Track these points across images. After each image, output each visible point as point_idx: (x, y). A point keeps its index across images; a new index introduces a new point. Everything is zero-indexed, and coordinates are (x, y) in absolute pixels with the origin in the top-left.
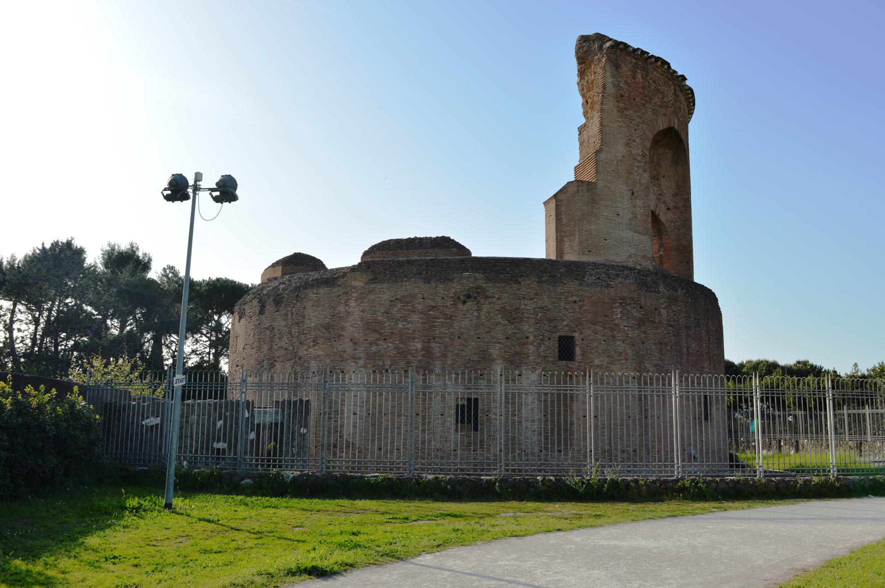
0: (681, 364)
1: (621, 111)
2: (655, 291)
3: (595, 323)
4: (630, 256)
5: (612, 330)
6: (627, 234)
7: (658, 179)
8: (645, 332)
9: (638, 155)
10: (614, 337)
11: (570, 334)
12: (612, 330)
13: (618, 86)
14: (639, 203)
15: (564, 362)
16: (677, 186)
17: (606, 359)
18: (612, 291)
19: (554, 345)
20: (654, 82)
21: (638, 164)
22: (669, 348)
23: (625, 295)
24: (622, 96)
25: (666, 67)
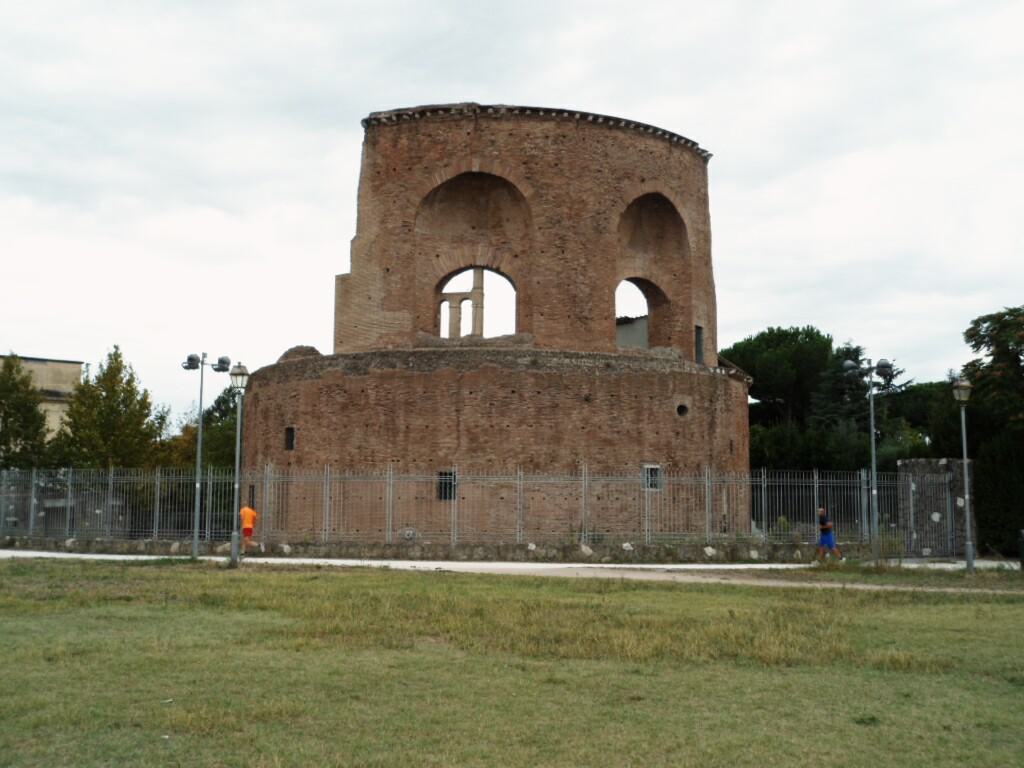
0: (394, 443)
1: (376, 189)
2: (365, 374)
3: (306, 413)
4: (380, 338)
5: (319, 418)
6: (377, 316)
7: (501, 226)
8: (347, 416)
9: (395, 228)
10: (319, 424)
11: (290, 426)
12: (319, 418)
13: (375, 163)
14: (395, 278)
15: (286, 452)
16: (527, 226)
17: (314, 446)
18: (320, 381)
19: (282, 436)
20: (430, 136)
21: (396, 238)
22: (376, 428)
23: (330, 382)
24: (379, 173)
25: (441, 112)
